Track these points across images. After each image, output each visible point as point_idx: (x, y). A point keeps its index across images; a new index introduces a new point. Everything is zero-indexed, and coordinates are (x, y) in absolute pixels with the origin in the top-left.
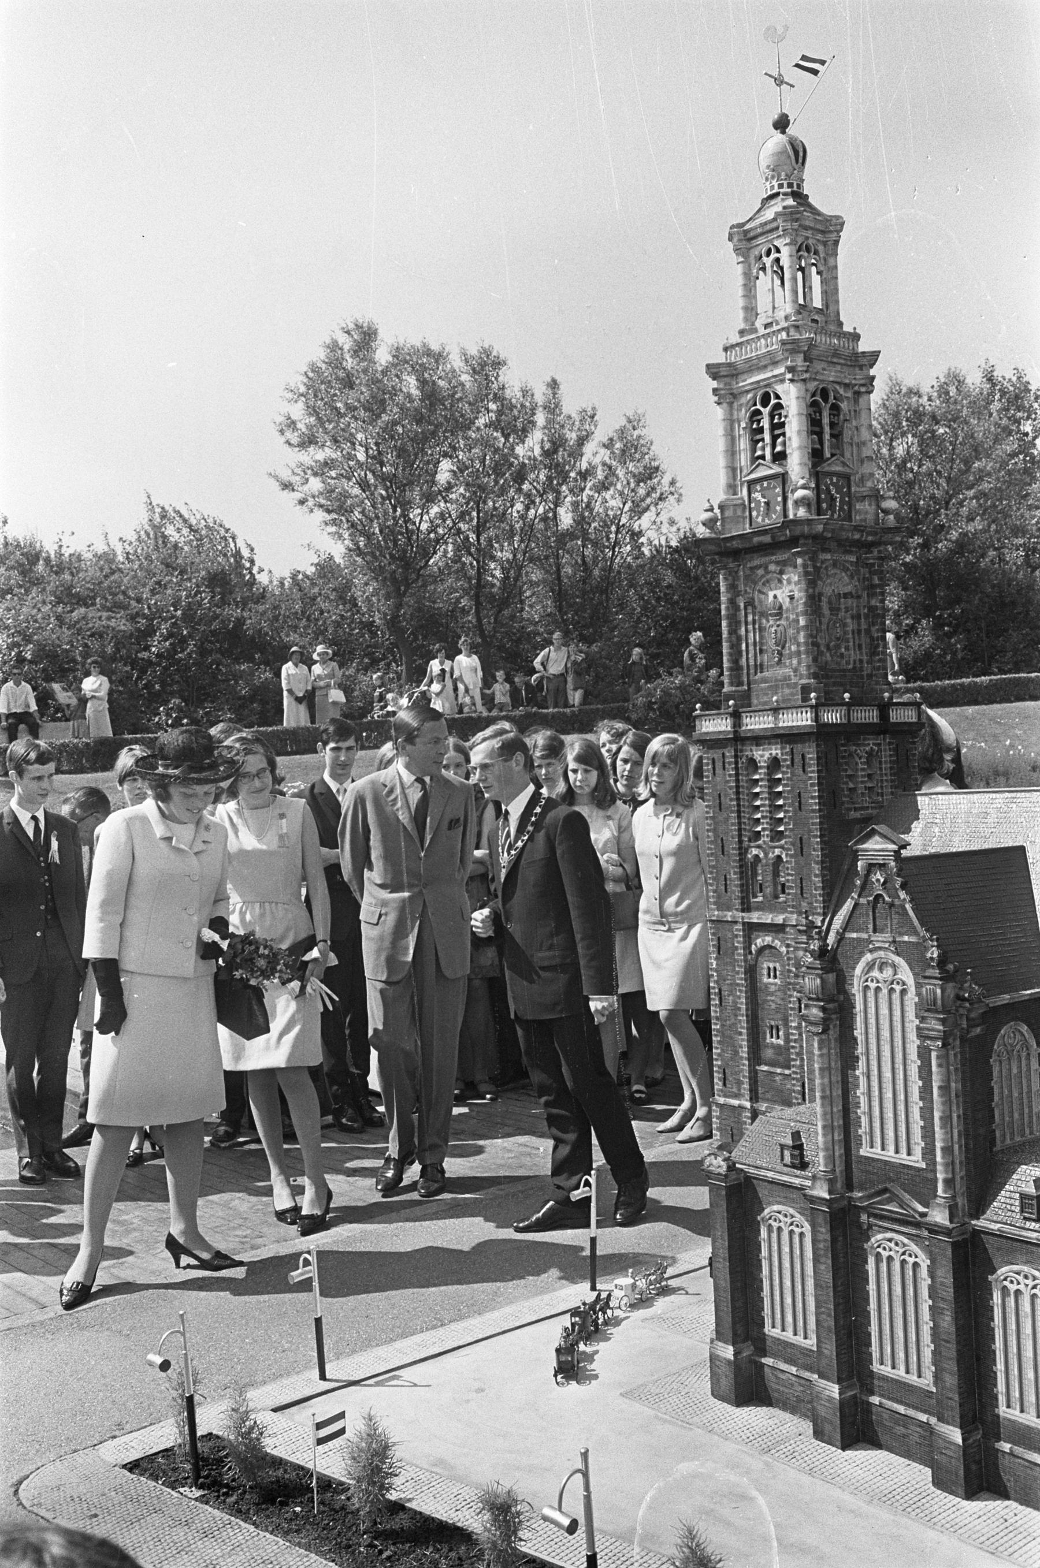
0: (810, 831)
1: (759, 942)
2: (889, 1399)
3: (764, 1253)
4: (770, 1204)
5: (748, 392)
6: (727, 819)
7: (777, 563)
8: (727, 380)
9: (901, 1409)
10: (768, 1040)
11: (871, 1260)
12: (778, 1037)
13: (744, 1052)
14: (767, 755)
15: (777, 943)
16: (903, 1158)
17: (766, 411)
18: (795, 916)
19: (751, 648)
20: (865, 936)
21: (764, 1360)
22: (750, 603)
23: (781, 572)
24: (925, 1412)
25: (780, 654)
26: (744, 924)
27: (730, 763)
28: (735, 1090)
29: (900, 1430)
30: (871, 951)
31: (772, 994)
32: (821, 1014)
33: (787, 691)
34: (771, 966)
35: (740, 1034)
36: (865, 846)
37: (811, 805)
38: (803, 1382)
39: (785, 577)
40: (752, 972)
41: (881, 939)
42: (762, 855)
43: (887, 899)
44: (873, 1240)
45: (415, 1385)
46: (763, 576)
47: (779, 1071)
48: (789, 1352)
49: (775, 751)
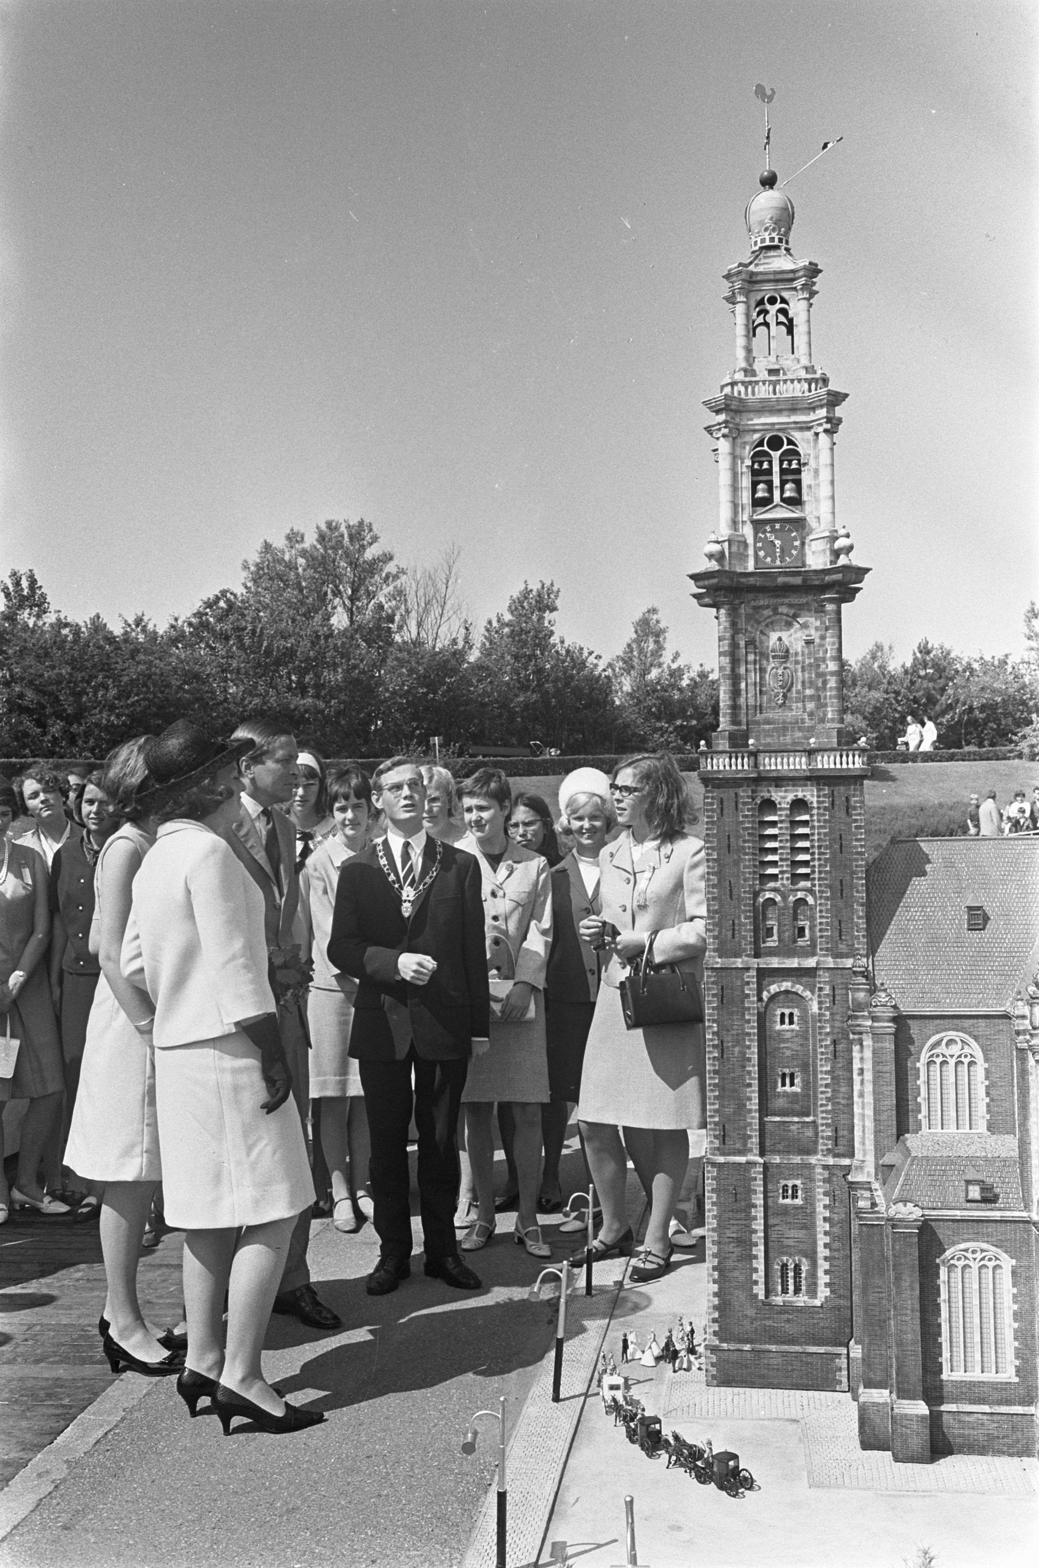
0: (853, 873)
1: (774, 988)
3: (944, 1295)
4: (954, 1244)
5: (755, 431)
6: (737, 863)
8: (732, 414)
10: (780, 1089)
13: (754, 1104)
14: (790, 797)
15: (799, 988)
17: (776, 455)
18: (830, 959)
19: (751, 688)
21: (943, 1408)
22: (751, 643)
23: (795, 617)
25: (785, 696)
26: (759, 970)
27: (745, 803)
28: (738, 1146)
31: (787, 1041)
34: (787, 1012)
35: (750, 1085)
37: (856, 847)
38: (995, 1418)
39: (801, 620)
40: (762, 1019)
42: (778, 899)
46: (769, 617)
48: (973, 1392)
49: (810, 794)
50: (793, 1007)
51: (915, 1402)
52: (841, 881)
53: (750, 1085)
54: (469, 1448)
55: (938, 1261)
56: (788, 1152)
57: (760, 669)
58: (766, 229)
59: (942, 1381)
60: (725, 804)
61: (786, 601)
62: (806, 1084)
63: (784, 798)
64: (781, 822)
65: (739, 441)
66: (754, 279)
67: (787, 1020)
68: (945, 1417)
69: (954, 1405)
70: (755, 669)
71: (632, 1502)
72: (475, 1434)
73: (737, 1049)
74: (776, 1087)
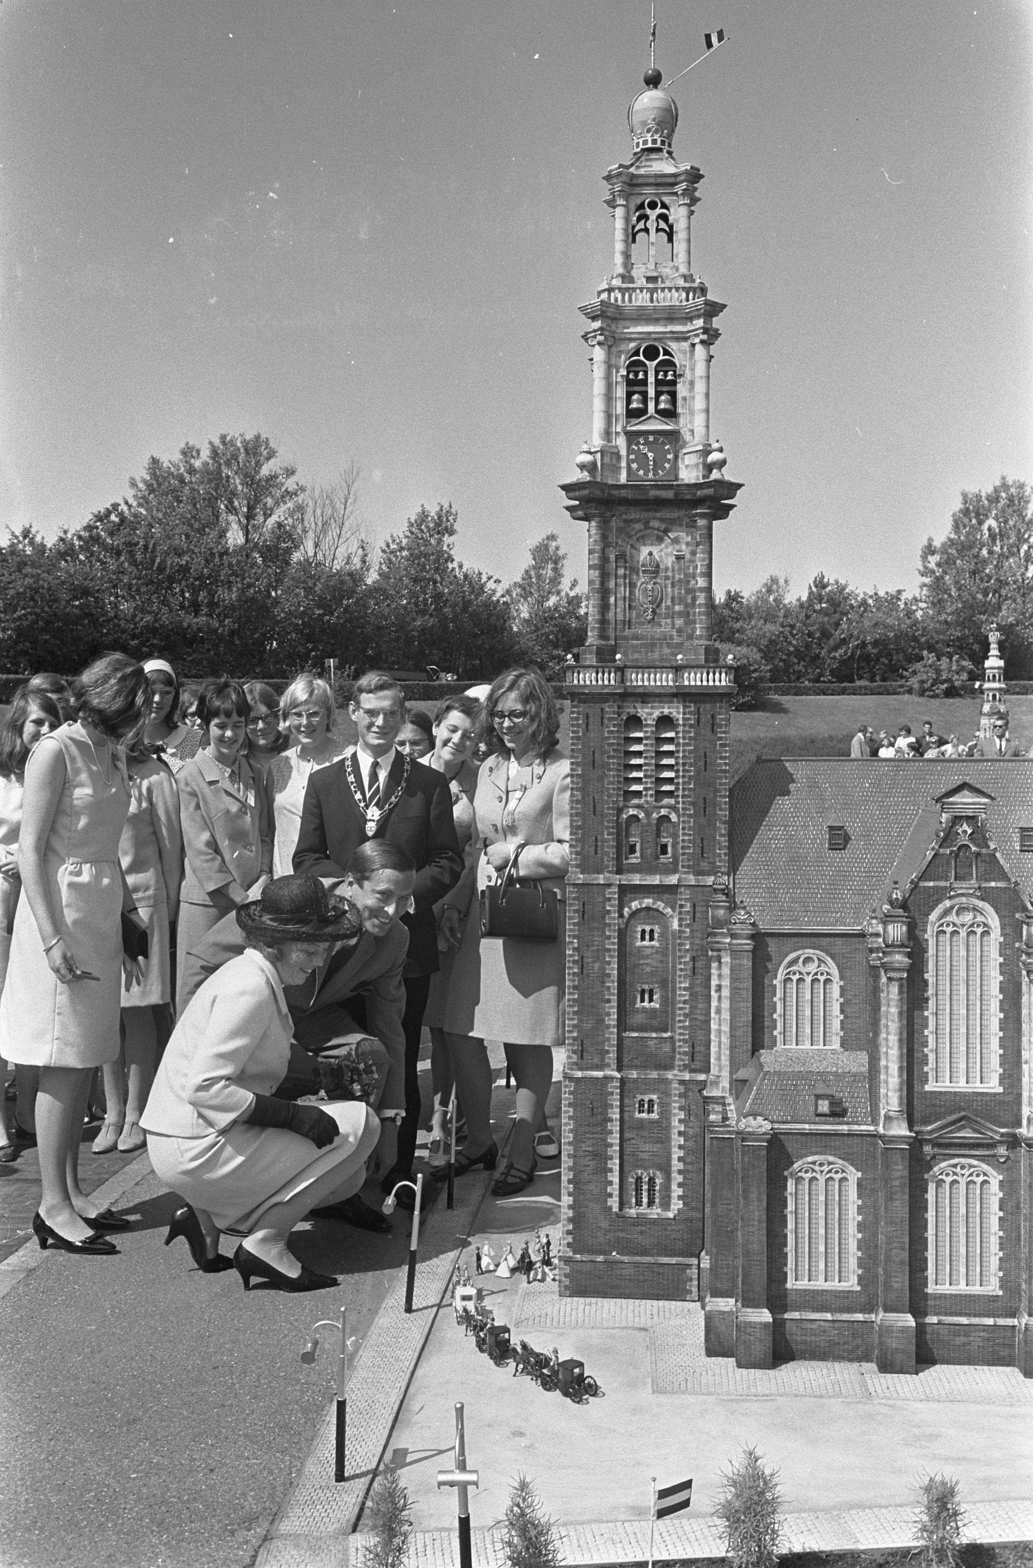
0: (716, 791)
1: (635, 905)
2: (946, 1315)
3: (791, 1206)
4: (802, 1157)
5: (631, 340)
6: (601, 779)
7: (662, 520)
9: (964, 1320)
10: (638, 1005)
11: (932, 1187)
12: (651, 1000)
13: (612, 1019)
14: (657, 713)
15: (660, 905)
16: (977, 1087)
18: (691, 877)
19: (620, 603)
20: (942, 884)
21: (786, 1316)
22: (621, 557)
23: (666, 531)
24: (988, 1316)
25: (654, 612)
26: (620, 886)
27: (610, 719)
28: (596, 1061)
29: (959, 1340)
30: (950, 898)
31: (647, 957)
32: (906, 960)
33: (667, 651)
34: (648, 928)
35: (609, 1001)
36: (951, 799)
37: (720, 765)
38: (837, 1325)
39: (672, 535)
40: (623, 935)
41: (962, 887)
42: (642, 815)
43: (974, 849)
44: (936, 1169)
45: (441, 1452)
46: (641, 531)
47: (654, 1035)
48: (817, 1300)
49: (676, 711)
50: (652, 924)
51: (759, 1310)
52: (705, 799)
53: (609, 1001)
54: (308, 1358)
55: (786, 1173)
56: (646, 1067)
57: (630, 583)
58: (648, 131)
59: (786, 1289)
60: (591, 719)
61: (658, 515)
62: (664, 1000)
63: (651, 714)
64: (647, 738)
65: (614, 349)
66: (635, 181)
67: (647, 937)
68: (788, 1324)
69: (798, 1313)
70: (625, 584)
71: (462, 1408)
72: (316, 1343)
73: (597, 965)
74: (635, 1003)
